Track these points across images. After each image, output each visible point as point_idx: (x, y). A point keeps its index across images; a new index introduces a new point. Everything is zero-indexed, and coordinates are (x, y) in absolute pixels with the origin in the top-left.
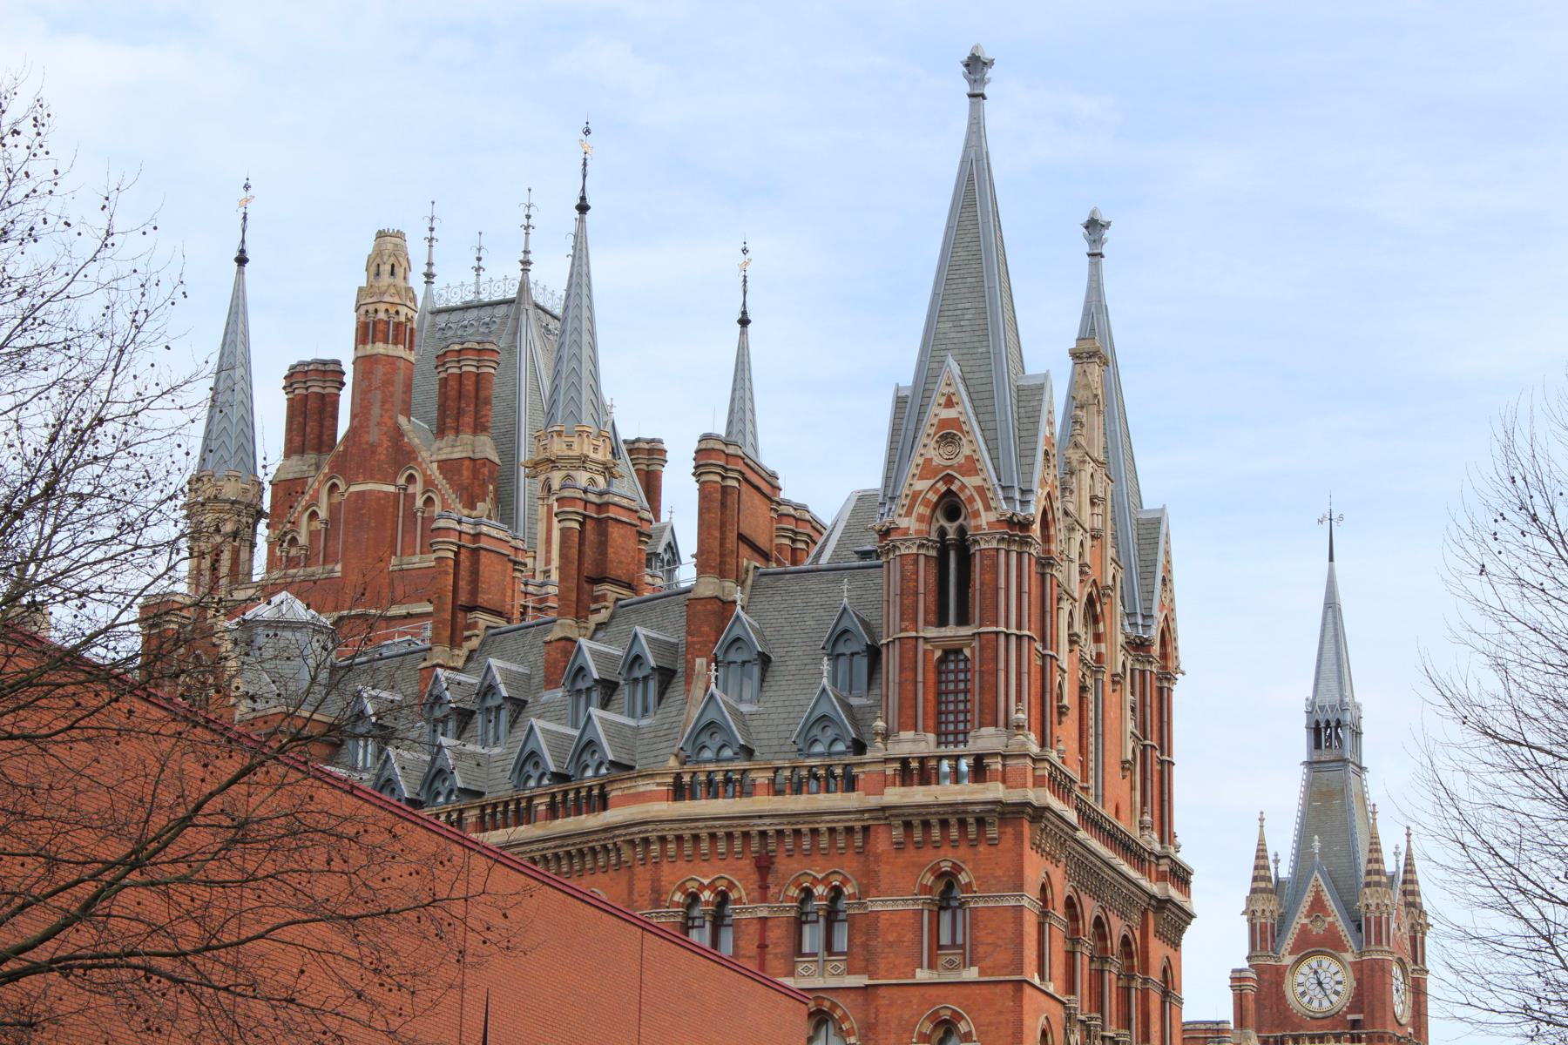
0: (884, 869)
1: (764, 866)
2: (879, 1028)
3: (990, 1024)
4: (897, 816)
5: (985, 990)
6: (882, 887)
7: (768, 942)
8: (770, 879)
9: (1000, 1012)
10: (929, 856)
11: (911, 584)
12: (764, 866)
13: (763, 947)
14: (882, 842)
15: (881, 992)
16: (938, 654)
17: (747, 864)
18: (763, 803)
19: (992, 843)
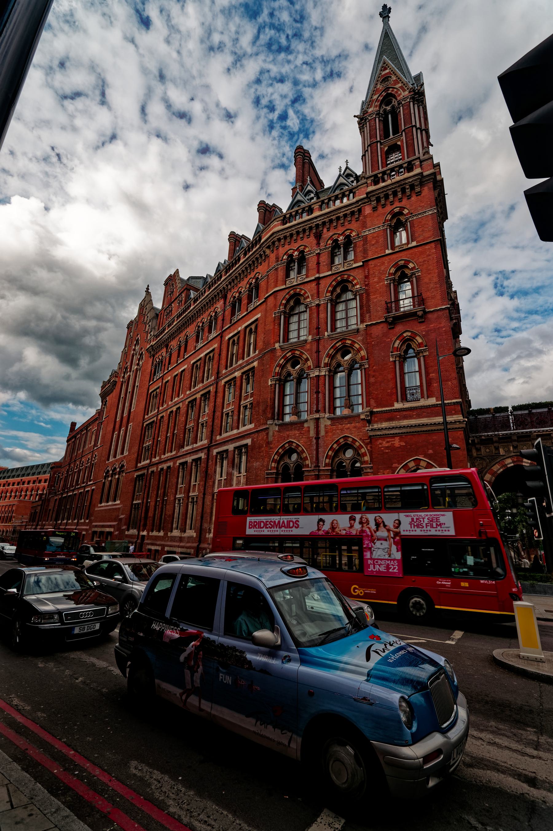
0: (368, 220)
1: (318, 237)
2: (370, 276)
3: (424, 261)
4: (374, 195)
5: (420, 249)
6: (368, 226)
7: (320, 262)
8: (321, 242)
9: (429, 255)
10: (389, 208)
11: (374, 127)
12: (318, 237)
13: (318, 263)
14: (368, 210)
15: (370, 263)
16: (386, 148)
17: (312, 239)
18: (316, 213)
19: (419, 194)
